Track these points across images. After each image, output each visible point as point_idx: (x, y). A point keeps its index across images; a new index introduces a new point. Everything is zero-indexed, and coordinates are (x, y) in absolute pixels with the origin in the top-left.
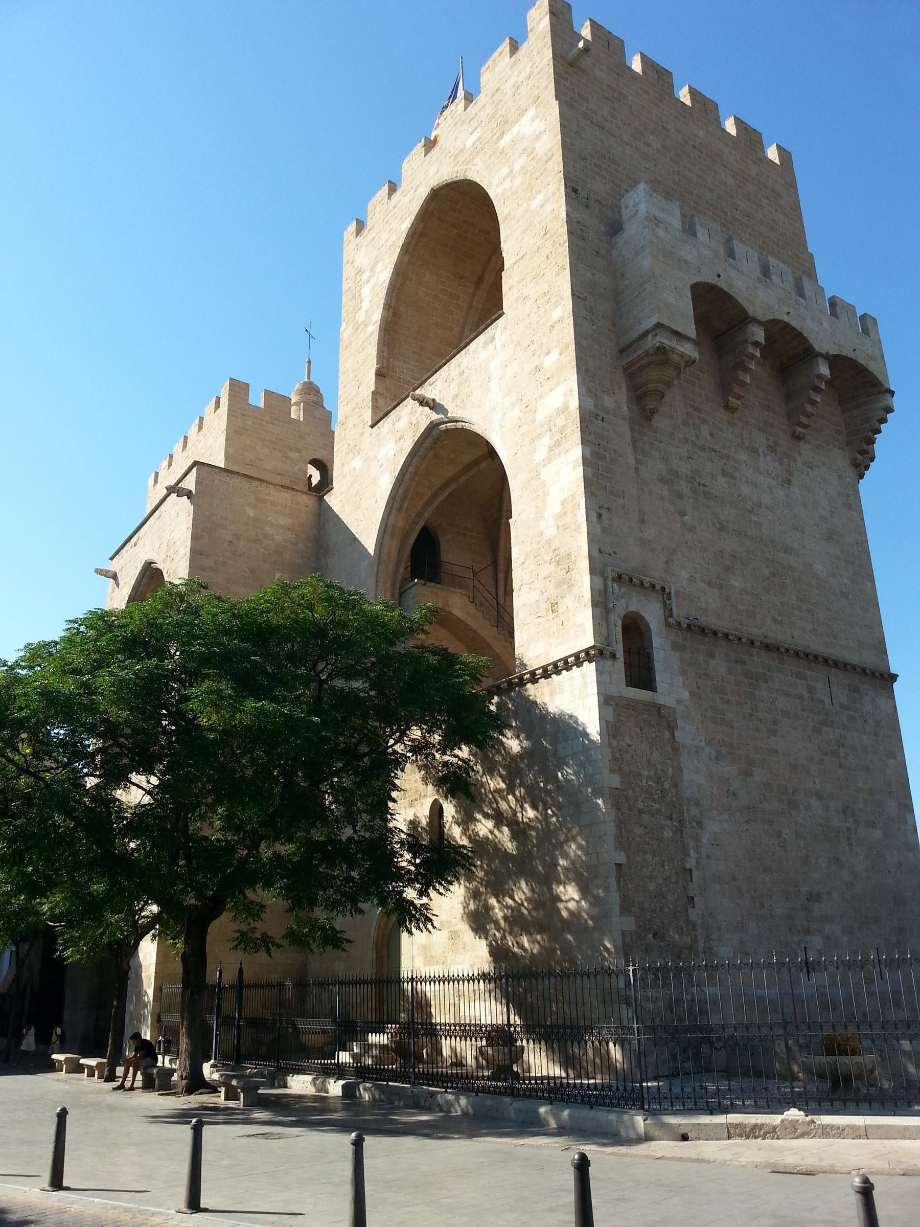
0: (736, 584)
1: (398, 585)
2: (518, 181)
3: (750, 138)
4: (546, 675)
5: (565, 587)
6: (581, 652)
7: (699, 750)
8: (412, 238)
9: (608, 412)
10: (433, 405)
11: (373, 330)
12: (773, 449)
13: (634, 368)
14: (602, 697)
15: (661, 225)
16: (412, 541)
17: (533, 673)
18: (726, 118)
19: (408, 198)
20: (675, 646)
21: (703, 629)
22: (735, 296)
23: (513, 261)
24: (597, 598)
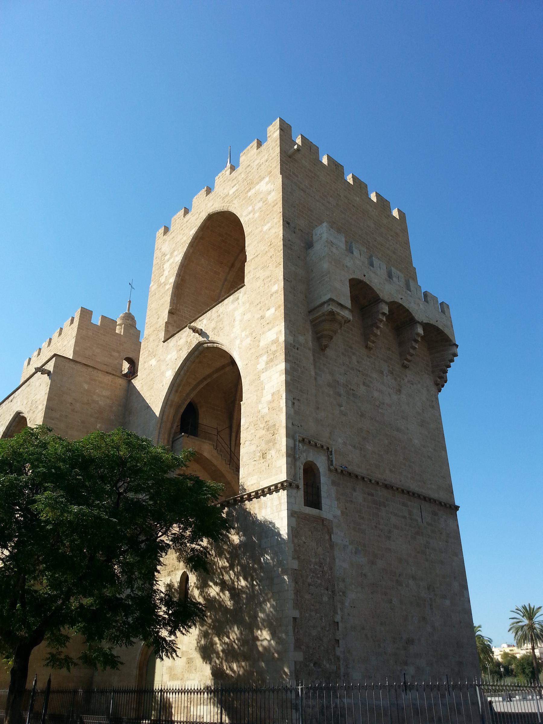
0: (370, 448)
1: (172, 436)
2: (257, 215)
3: (384, 205)
4: (257, 496)
5: (271, 444)
6: (279, 483)
7: (345, 547)
10: (201, 333)
13: (317, 321)
14: (290, 512)
16: (182, 410)
17: (249, 495)
18: (372, 192)
19: (195, 218)
20: (334, 483)
21: (350, 474)
24: (290, 452)
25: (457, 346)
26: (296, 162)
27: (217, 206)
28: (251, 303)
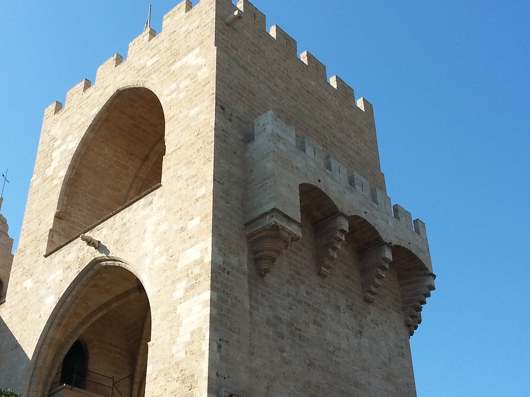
2: (182, 95)
3: (346, 92)
8: (98, 121)
9: (233, 268)
10: (99, 246)
12: (350, 308)
13: (255, 237)
15: (281, 141)
16: (65, 352)
18: (331, 76)
19: (99, 93)
23: (173, 150)
25: (434, 276)
26: (236, 33)
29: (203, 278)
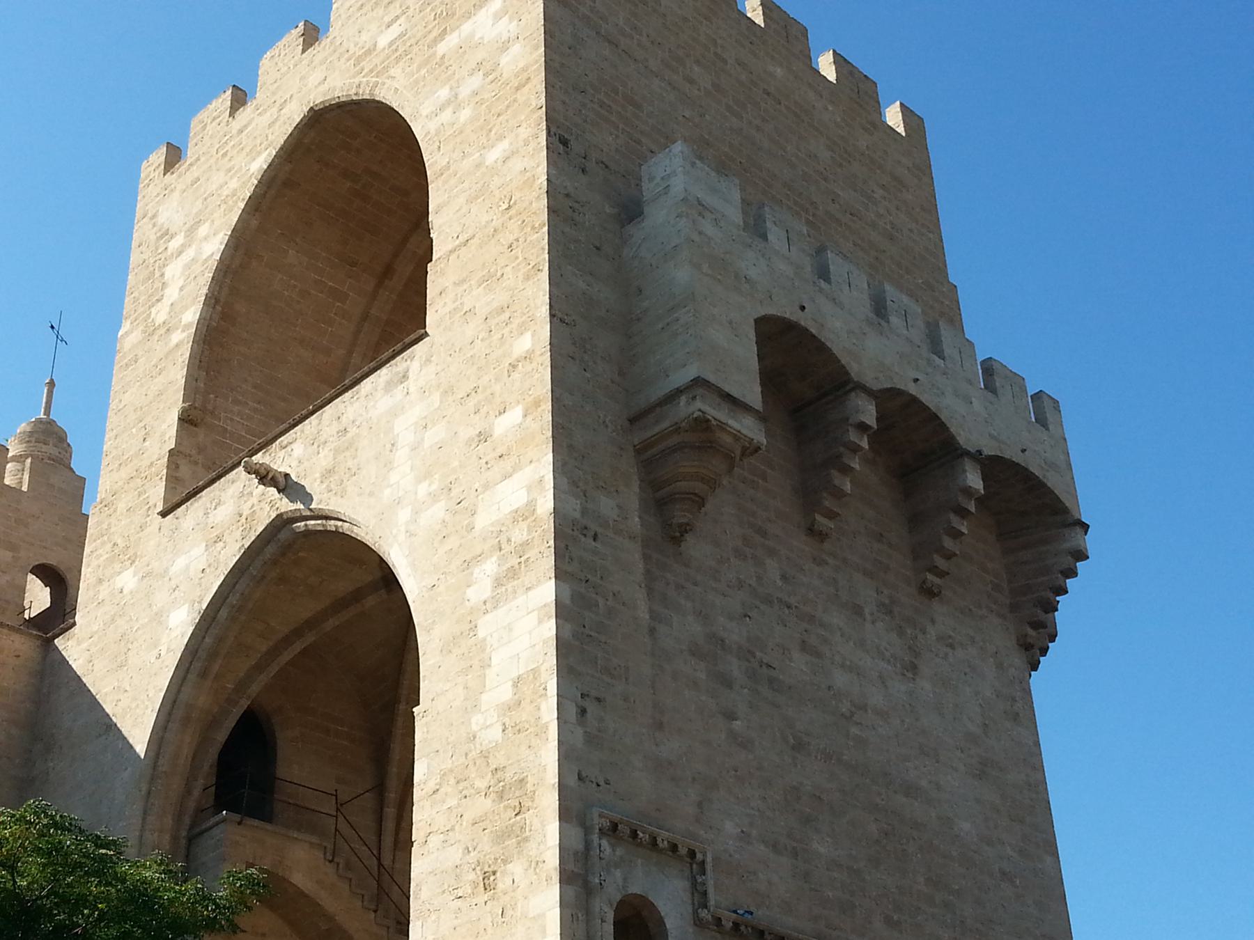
0: (822, 850)
1: (187, 820)
2: (465, 114)
10: (286, 485)
11: (182, 339)
12: (887, 609)
13: (655, 450)
15: (707, 214)
16: (222, 736)
18: (821, 52)
22: (829, 344)
23: (450, 247)
24: (570, 866)
27: (339, 84)
28: (449, 391)
29: (537, 550)
